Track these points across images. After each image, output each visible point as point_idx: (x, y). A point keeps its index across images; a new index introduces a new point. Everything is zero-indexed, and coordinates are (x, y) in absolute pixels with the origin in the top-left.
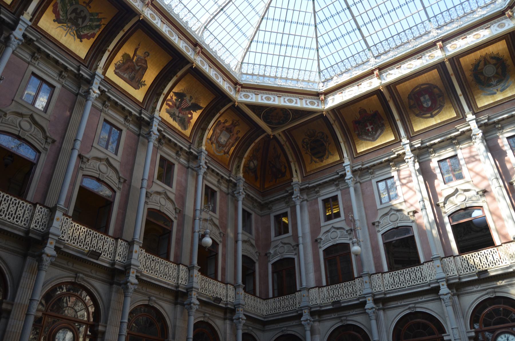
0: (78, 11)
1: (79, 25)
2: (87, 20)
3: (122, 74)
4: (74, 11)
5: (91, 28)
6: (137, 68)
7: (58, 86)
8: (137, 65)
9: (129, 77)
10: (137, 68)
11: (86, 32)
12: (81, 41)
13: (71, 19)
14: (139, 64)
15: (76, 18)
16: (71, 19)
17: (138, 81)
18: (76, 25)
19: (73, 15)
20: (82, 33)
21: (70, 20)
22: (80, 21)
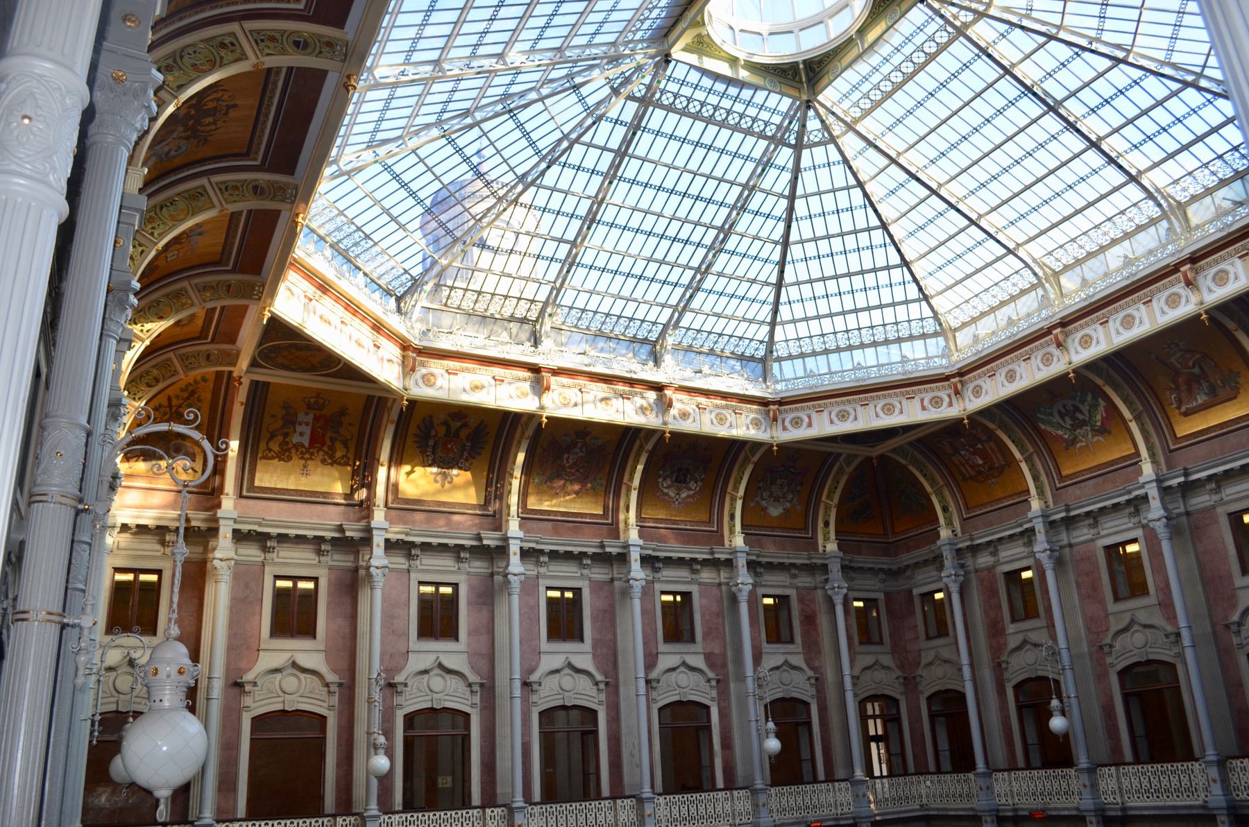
0: (1063, 411)
1: (1084, 420)
2: (1081, 406)
3: (1195, 404)
4: (1062, 416)
5: (1094, 407)
6: (1196, 370)
7: (1138, 533)
8: (1189, 368)
9: (1206, 394)
10: (1196, 370)
11: (1099, 417)
12: (1110, 432)
13: (1071, 425)
14: (1190, 364)
15: (1074, 418)
16: (1071, 425)
17: (1223, 383)
18: (1083, 423)
19: (1067, 419)
20: (1099, 424)
21: (1074, 427)
22: (1079, 415)
